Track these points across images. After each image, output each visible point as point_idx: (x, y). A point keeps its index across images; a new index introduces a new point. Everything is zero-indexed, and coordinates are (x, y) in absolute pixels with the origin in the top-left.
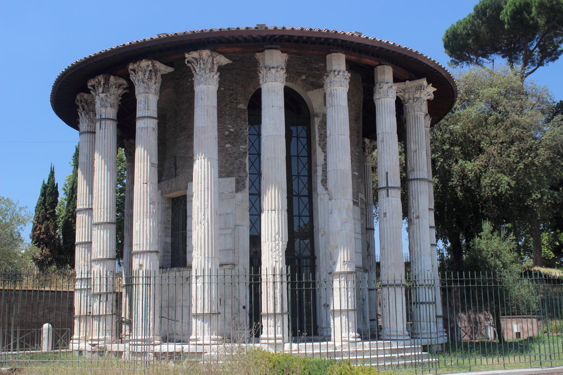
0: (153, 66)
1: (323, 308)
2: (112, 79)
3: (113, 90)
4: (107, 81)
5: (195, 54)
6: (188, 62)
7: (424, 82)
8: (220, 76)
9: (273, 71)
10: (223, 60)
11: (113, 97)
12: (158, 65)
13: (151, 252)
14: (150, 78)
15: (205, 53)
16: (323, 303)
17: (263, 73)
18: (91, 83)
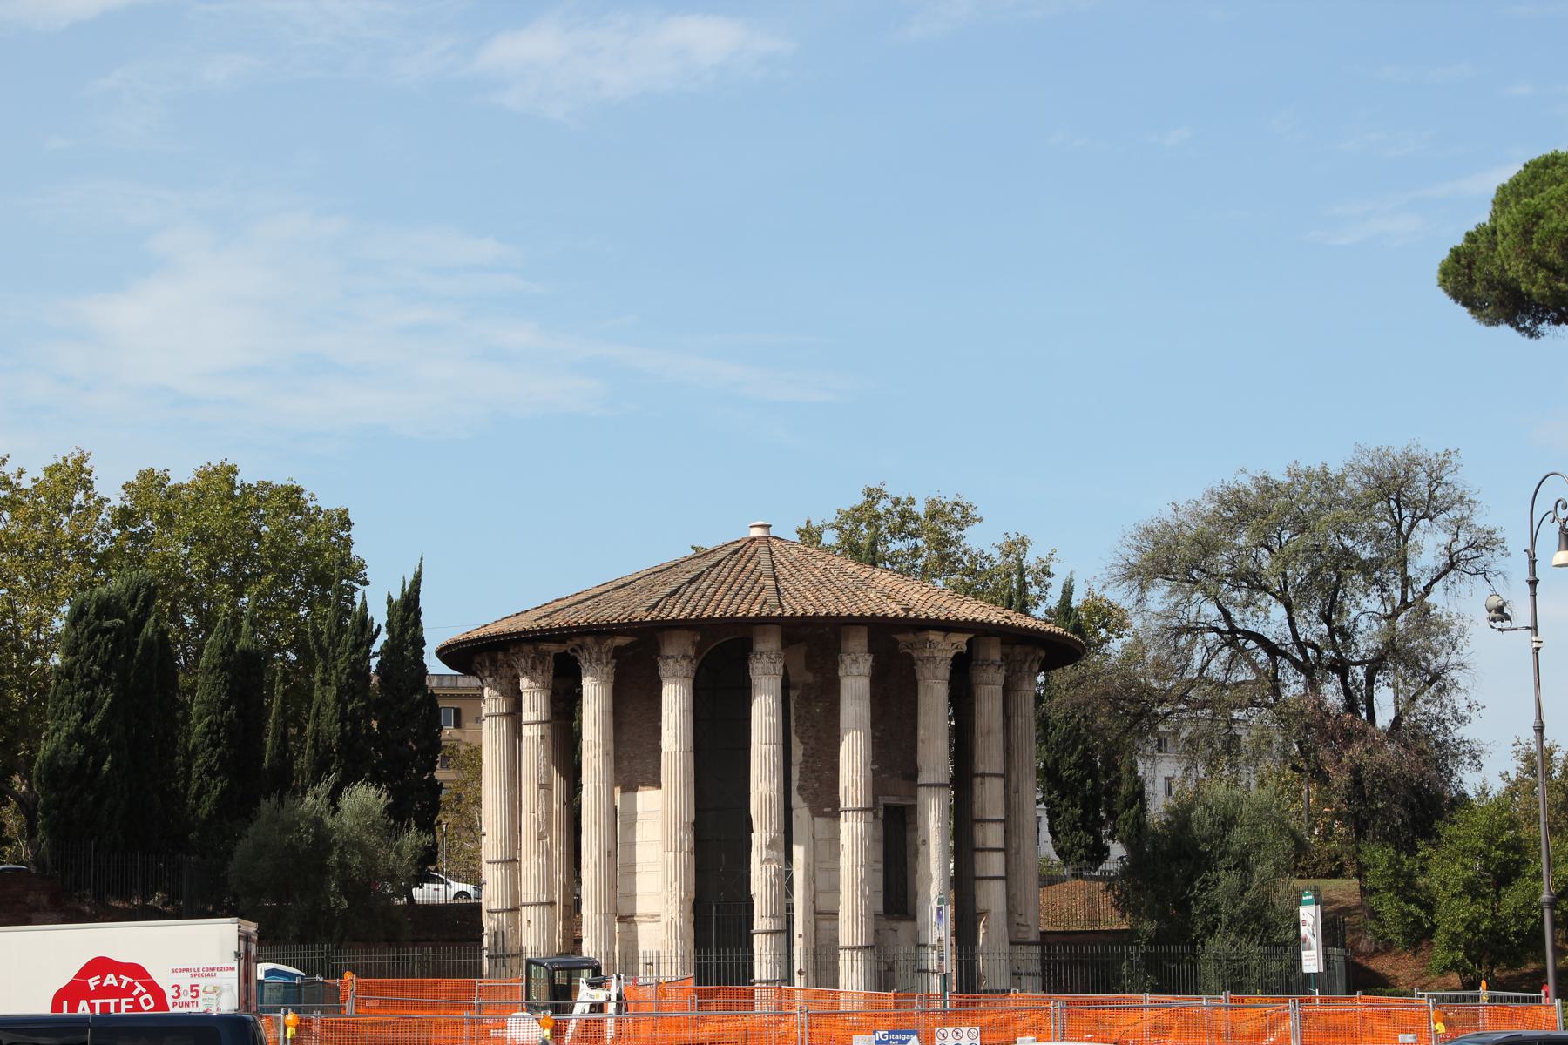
0: (536, 649)
1: (797, 976)
2: (500, 656)
3: (504, 671)
4: (494, 662)
5: (578, 641)
6: (573, 650)
7: (935, 636)
8: (616, 666)
9: (671, 662)
10: (620, 641)
11: (504, 682)
12: (544, 647)
13: (541, 904)
14: (534, 668)
15: (589, 640)
16: (797, 969)
17: (661, 663)
18: (477, 659)
